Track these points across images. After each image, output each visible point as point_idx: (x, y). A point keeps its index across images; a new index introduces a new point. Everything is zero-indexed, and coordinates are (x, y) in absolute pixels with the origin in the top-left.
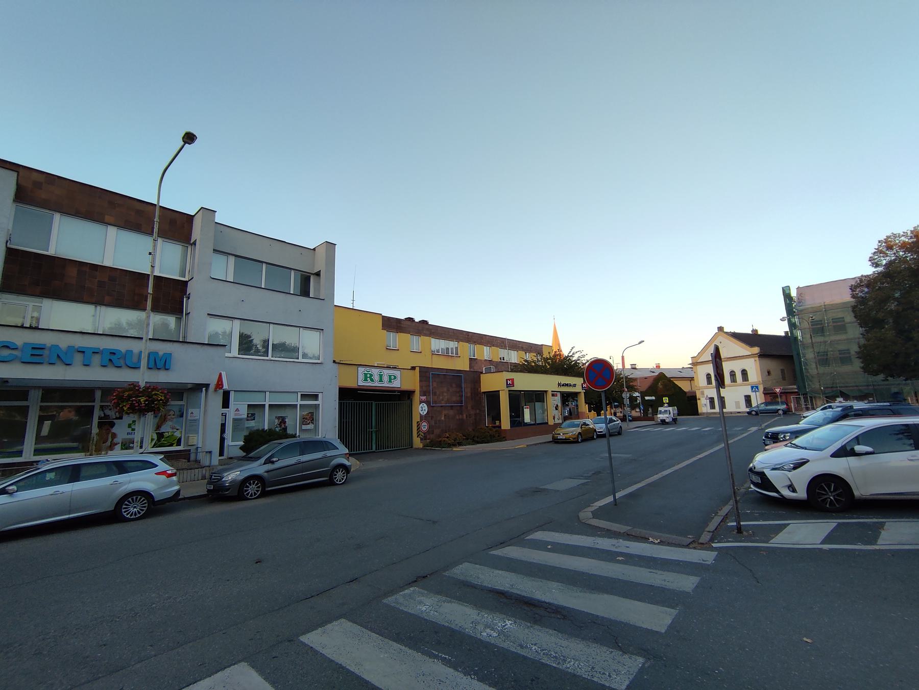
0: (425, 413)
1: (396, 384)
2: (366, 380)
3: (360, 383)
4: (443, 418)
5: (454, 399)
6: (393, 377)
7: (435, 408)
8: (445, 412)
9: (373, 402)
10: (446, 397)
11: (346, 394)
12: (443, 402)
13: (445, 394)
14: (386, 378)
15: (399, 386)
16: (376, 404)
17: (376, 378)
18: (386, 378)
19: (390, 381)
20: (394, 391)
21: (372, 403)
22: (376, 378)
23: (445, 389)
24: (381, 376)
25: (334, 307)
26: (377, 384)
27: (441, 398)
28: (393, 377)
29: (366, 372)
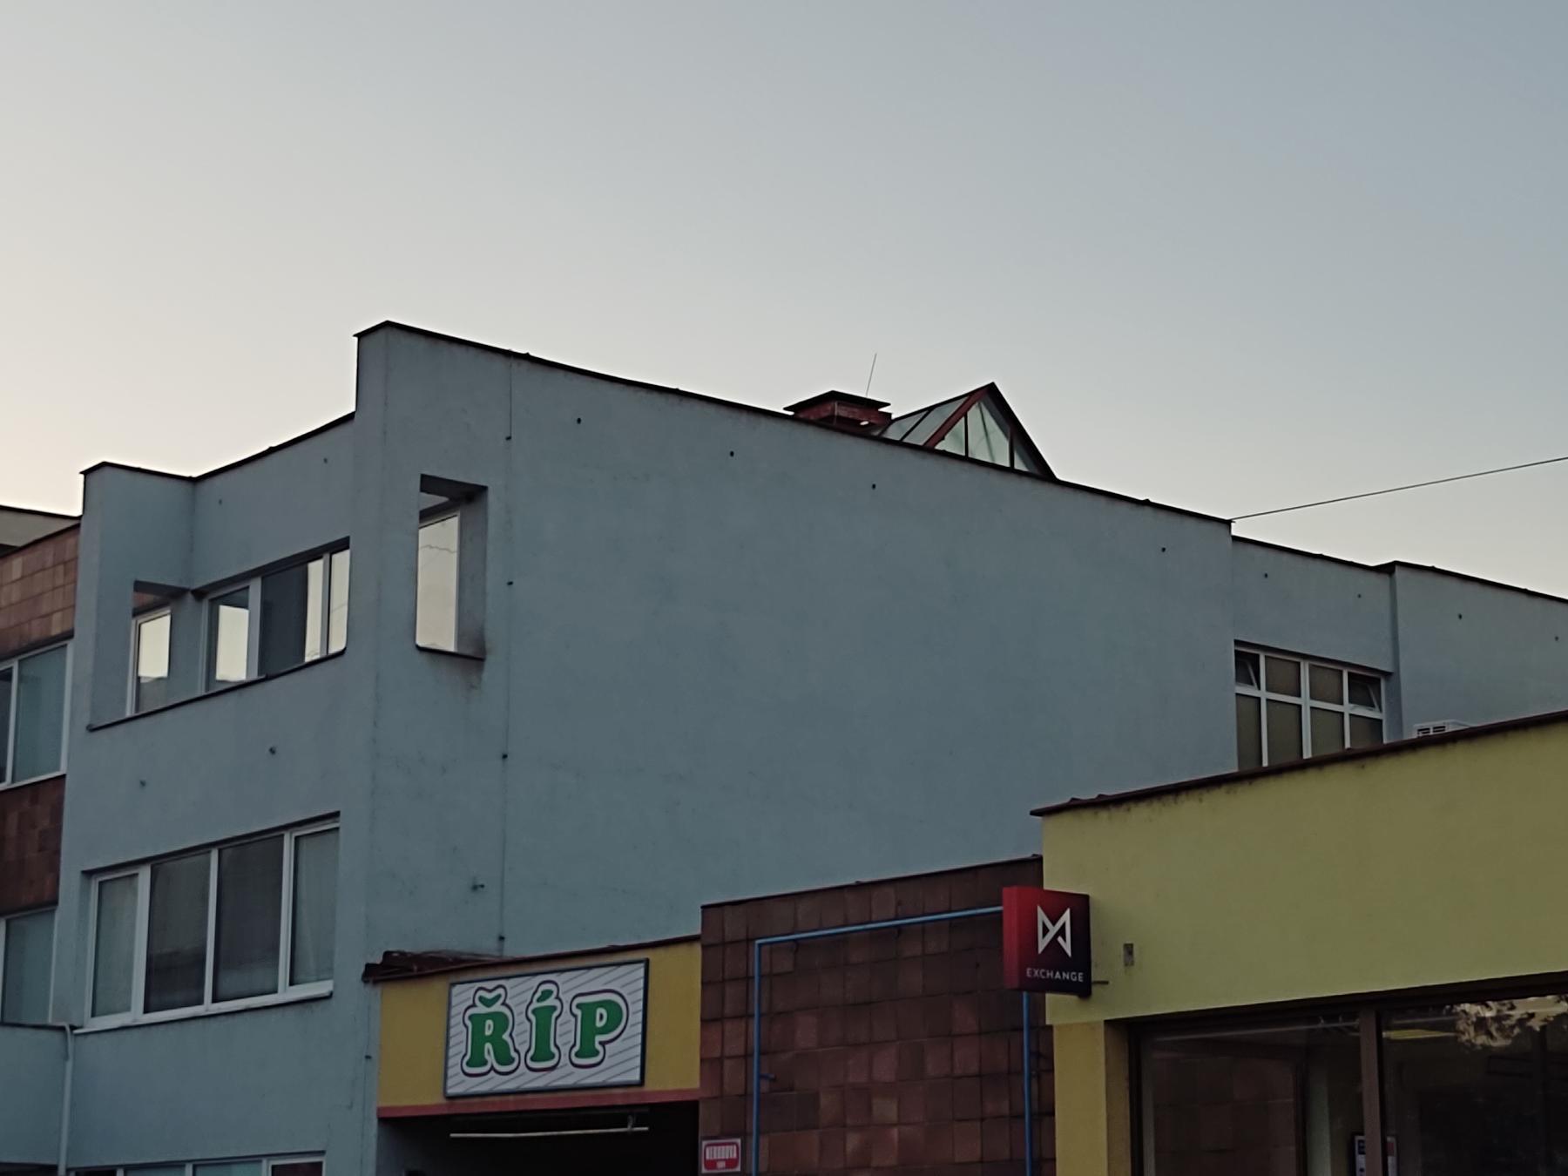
2: (477, 1059)
3: (459, 1084)
6: (601, 1018)
13: (886, 1109)
14: (566, 1032)
15: (636, 1076)
17: (522, 1037)
18: (566, 1032)
19: (587, 1050)
20: (615, 1115)
22: (522, 1037)
23: (885, 1067)
24: (544, 1019)
25: (417, 652)
27: (853, 1141)
28: (601, 1018)
29: (481, 1009)
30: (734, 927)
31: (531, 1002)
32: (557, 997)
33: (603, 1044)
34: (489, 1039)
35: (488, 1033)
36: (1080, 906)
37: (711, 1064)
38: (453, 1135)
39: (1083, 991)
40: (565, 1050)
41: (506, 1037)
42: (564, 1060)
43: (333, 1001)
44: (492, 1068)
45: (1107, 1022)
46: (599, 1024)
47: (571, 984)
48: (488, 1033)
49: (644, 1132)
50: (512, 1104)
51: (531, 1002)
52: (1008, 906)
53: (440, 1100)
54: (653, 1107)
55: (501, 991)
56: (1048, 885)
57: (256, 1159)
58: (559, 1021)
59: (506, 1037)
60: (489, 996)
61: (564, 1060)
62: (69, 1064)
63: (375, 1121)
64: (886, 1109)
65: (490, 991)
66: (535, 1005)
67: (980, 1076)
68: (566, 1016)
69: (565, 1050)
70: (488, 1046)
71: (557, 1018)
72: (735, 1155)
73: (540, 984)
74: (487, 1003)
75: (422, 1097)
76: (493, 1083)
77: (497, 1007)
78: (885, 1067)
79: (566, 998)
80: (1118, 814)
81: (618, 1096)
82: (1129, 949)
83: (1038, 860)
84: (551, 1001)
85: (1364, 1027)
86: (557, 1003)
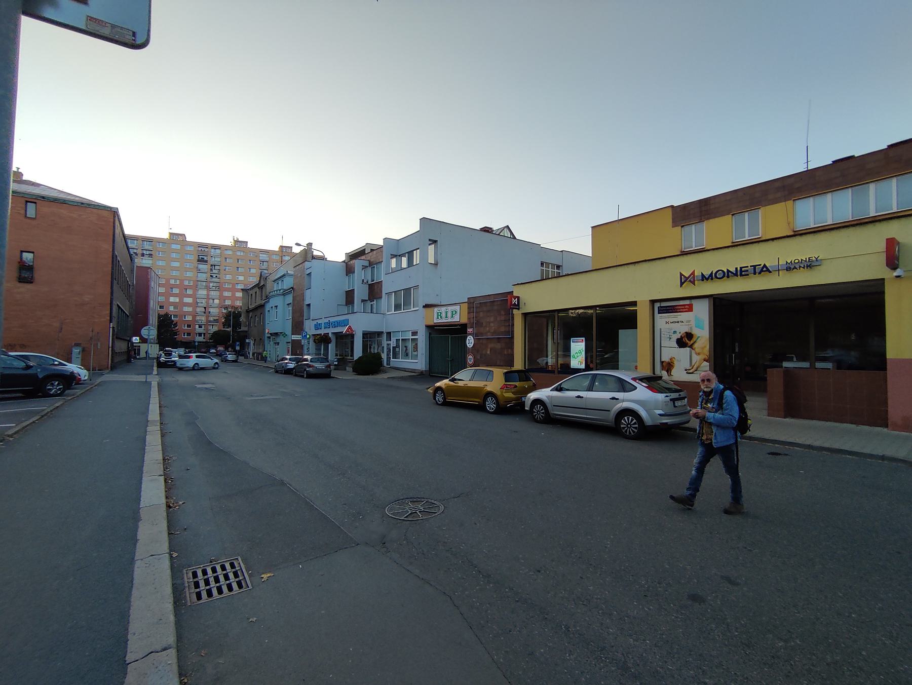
0: (472, 345)
1: (456, 319)
2: (438, 318)
4: (488, 352)
5: (503, 329)
6: (454, 313)
7: (481, 341)
8: (491, 345)
10: (493, 328)
11: (431, 328)
12: (489, 334)
13: (492, 325)
14: (449, 314)
17: (444, 315)
18: (449, 314)
19: (452, 317)
22: (444, 315)
23: (492, 319)
24: (446, 312)
27: (487, 329)
28: (454, 313)
29: (438, 311)
30: (472, 301)
36: (518, 298)
37: (469, 319)
39: (519, 309)
45: (522, 314)
47: (450, 308)
52: (509, 298)
54: (461, 324)
56: (514, 295)
64: (492, 325)
67: (505, 320)
75: (431, 323)
78: (492, 319)
80: (524, 285)
81: (456, 323)
82: (525, 303)
83: (513, 292)
85: (556, 314)
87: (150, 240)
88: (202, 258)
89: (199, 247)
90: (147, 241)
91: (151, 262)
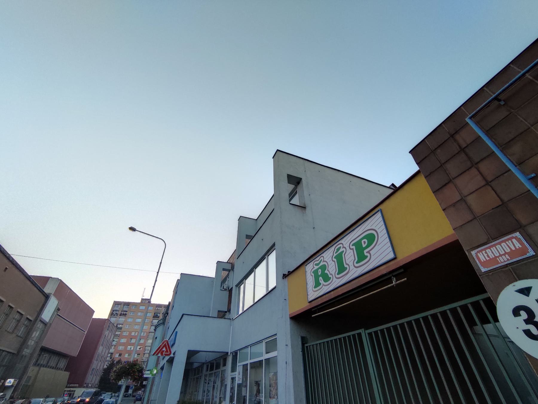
2: (317, 284)
3: (312, 295)
9: (361, 331)
14: (350, 257)
15: (391, 256)
16: (370, 334)
20: (383, 279)
21: (360, 335)
22: (332, 268)
26: (336, 282)
31: (333, 255)
32: (343, 247)
33: (368, 252)
34: (320, 276)
35: (319, 274)
38: (312, 316)
40: (351, 264)
41: (326, 272)
42: (352, 267)
43: (276, 288)
44: (323, 285)
46: (364, 246)
47: (346, 241)
48: (319, 274)
49: (405, 281)
50: (333, 295)
51: (333, 255)
53: (308, 304)
55: (322, 258)
57: (260, 342)
58: (346, 255)
59: (326, 272)
60: (318, 262)
61: (352, 267)
62: (232, 327)
63: (289, 319)
65: (318, 260)
66: (335, 255)
68: (349, 251)
69: (351, 264)
70: (321, 278)
71: (344, 255)
72: (518, 245)
73: (335, 247)
74: (316, 265)
75: (301, 306)
76: (325, 289)
77: (322, 264)
79: (347, 246)
81: (383, 270)
84: (341, 250)
86: (344, 249)
87: (128, 304)
88: (156, 315)
89: (156, 307)
90: (126, 305)
91: (124, 319)
